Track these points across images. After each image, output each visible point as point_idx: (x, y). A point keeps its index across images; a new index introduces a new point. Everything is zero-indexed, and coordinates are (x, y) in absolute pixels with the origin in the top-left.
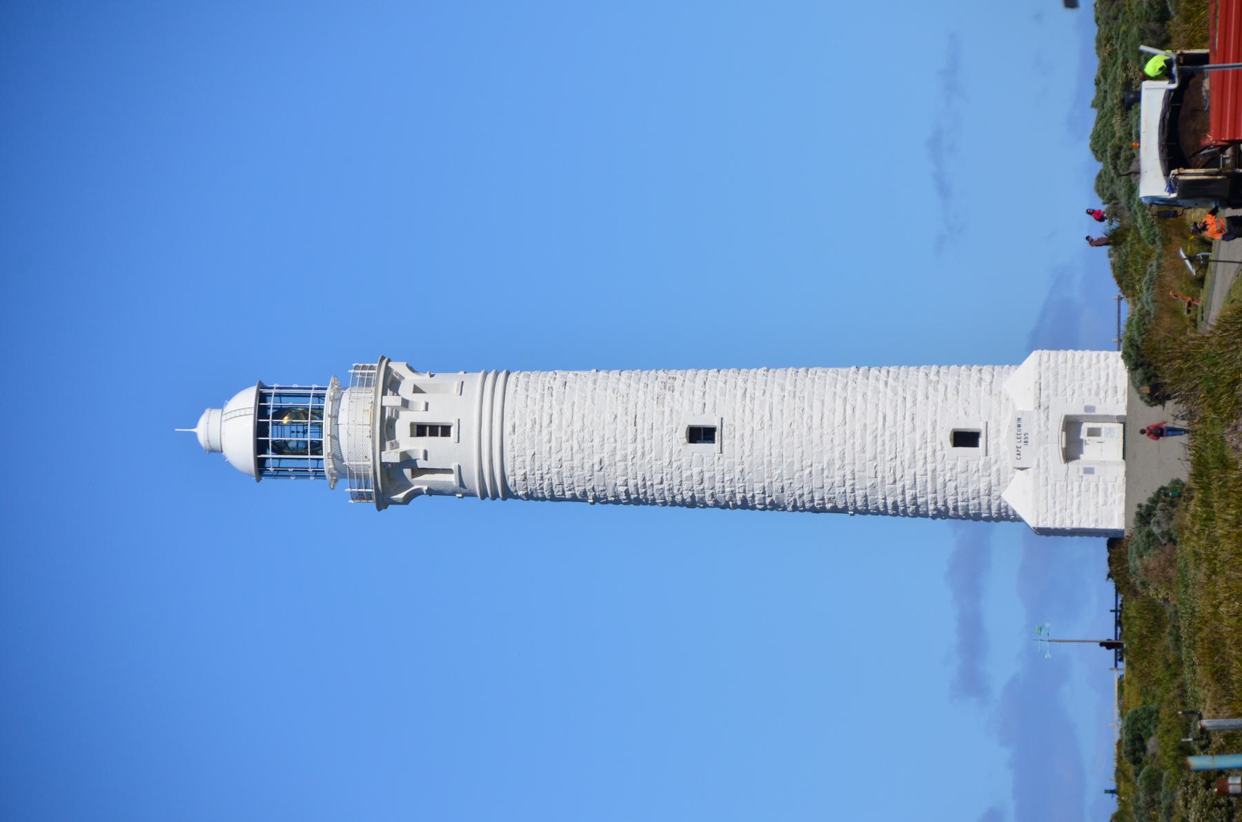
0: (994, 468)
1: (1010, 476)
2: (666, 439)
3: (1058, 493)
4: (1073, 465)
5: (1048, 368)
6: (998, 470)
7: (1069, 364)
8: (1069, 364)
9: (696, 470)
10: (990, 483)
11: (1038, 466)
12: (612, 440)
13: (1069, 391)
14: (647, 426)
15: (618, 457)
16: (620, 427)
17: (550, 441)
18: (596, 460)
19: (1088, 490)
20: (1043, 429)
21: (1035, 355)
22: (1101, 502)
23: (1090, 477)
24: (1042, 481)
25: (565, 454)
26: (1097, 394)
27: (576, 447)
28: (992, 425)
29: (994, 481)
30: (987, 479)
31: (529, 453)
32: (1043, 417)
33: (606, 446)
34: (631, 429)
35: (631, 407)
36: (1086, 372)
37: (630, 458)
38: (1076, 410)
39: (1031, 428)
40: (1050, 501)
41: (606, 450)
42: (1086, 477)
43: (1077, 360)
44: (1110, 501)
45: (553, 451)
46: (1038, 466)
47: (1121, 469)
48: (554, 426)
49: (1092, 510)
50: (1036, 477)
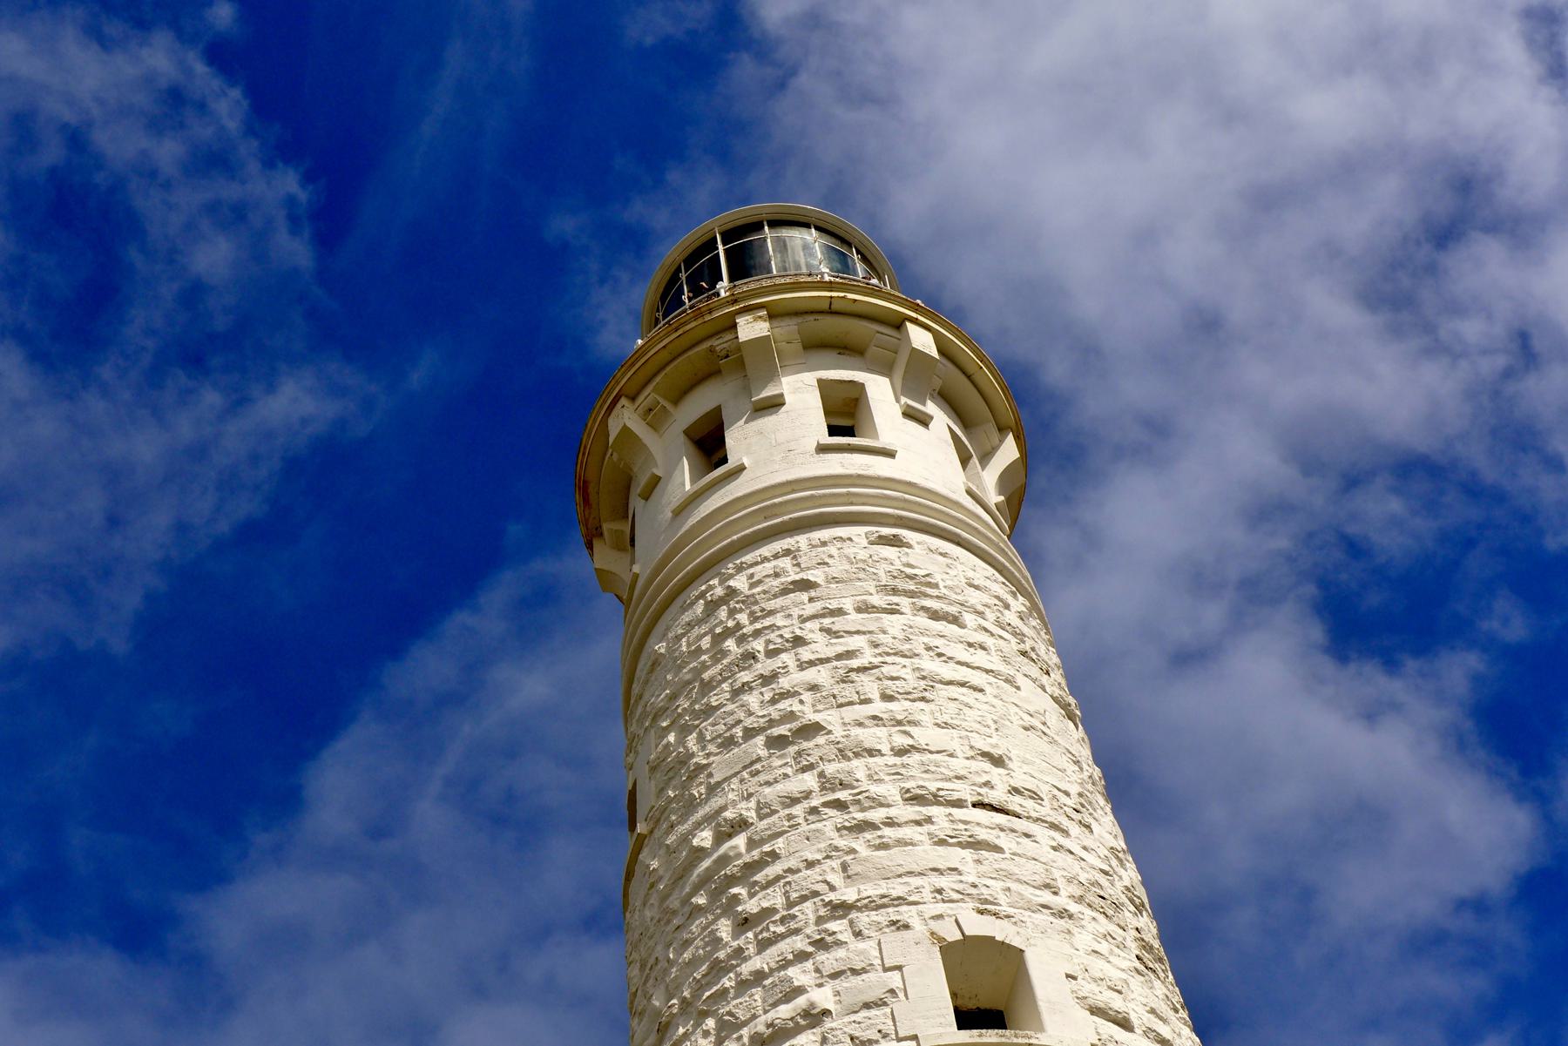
2: (943, 882)
9: (823, 997)
12: (901, 741)
14: (983, 834)
15: (830, 769)
16: (959, 765)
17: (865, 608)
18: (811, 716)
25: (821, 646)
27: (855, 663)
31: (816, 575)
33: (882, 732)
34: (965, 792)
35: (1045, 811)
37: (843, 795)
41: (856, 732)
45: (827, 621)
48: (923, 621)
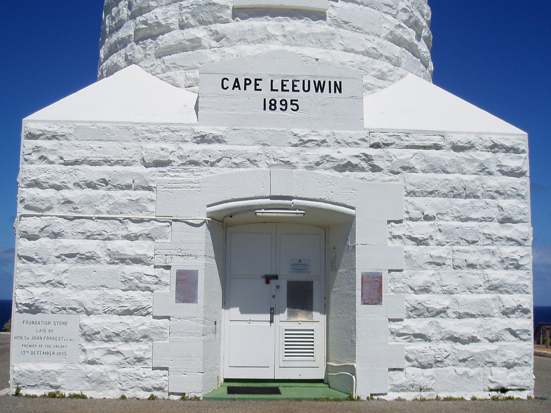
0: (199, 32)
1: (179, 75)
3: (119, 195)
4: (201, 240)
5: (484, 170)
6: (195, 44)
7: (494, 228)
8: (494, 228)
10: (168, 29)
11: (202, 139)
13: (422, 229)
19: (129, 284)
20: (314, 154)
21: (514, 135)
22: (91, 322)
23: (169, 291)
24: (154, 149)
26: (417, 312)
28: (319, 27)
29: (166, 40)
30: (174, 21)
32: (346, 154)
36: (474, 277)
38: (370, 252)
39: (315, 115)
40: (94, 173)
42: (169, 277)
43: (508, 250)
44: (95, 349)
46: (202, 139)
47: (196, 386)
49: (67, 296)
50: (170, 131)
